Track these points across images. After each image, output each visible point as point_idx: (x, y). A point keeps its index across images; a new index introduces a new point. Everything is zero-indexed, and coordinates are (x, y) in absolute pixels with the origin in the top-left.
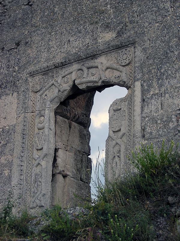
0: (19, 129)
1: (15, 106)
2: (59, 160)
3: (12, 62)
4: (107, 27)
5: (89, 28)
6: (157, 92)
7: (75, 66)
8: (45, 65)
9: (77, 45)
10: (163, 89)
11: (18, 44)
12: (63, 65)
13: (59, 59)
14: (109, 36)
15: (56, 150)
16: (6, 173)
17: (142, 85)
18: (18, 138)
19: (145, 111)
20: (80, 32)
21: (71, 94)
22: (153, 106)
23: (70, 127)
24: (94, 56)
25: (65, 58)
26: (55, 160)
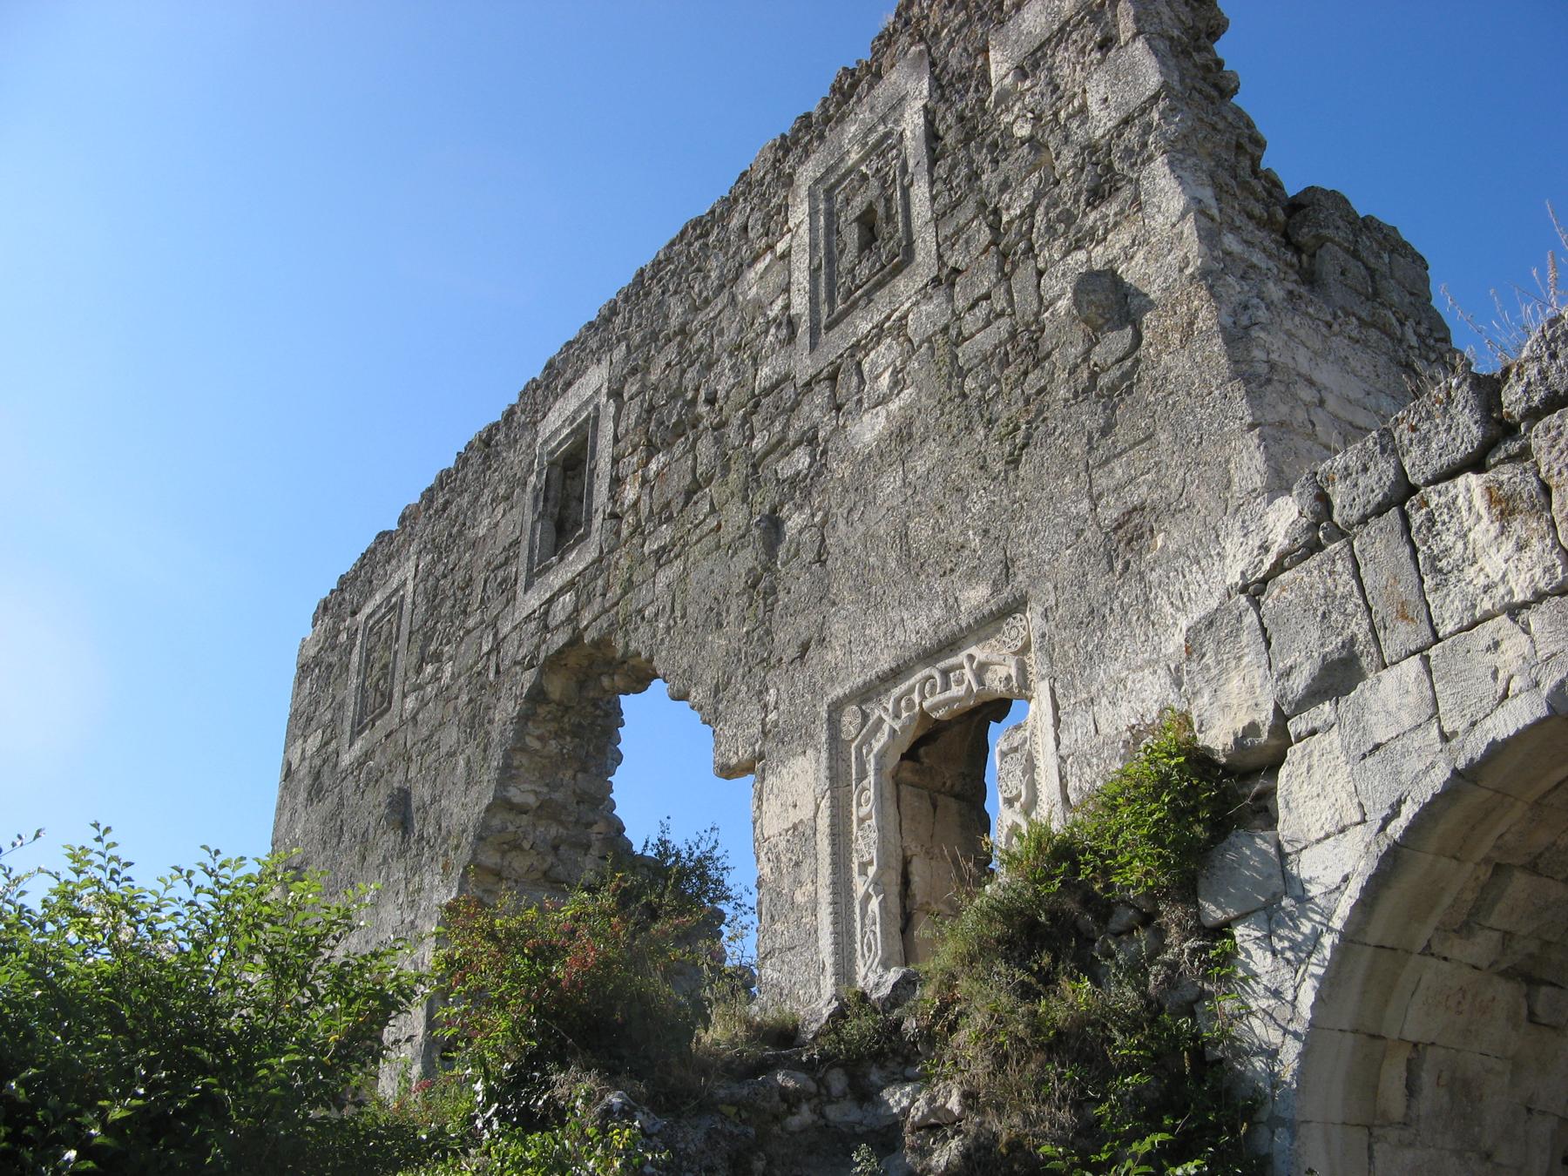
0: (824, 823)
1: (810, 778)
2: (916, 880)
3: (800, 685)
4: (972, 575)
6: (1084, 696)
8: (860, 681)
10: (1094, 689)
11: (805, 647)
12: (896, 674)
13: (885, 663)
14: (976, 596)
15: (906, 863)
17: (1052, 690)
19: (1065, 740)
20: (921, 598)
21: (920, 733)
23: (935, 807)
25: (897, 658)
26: (906, 881)
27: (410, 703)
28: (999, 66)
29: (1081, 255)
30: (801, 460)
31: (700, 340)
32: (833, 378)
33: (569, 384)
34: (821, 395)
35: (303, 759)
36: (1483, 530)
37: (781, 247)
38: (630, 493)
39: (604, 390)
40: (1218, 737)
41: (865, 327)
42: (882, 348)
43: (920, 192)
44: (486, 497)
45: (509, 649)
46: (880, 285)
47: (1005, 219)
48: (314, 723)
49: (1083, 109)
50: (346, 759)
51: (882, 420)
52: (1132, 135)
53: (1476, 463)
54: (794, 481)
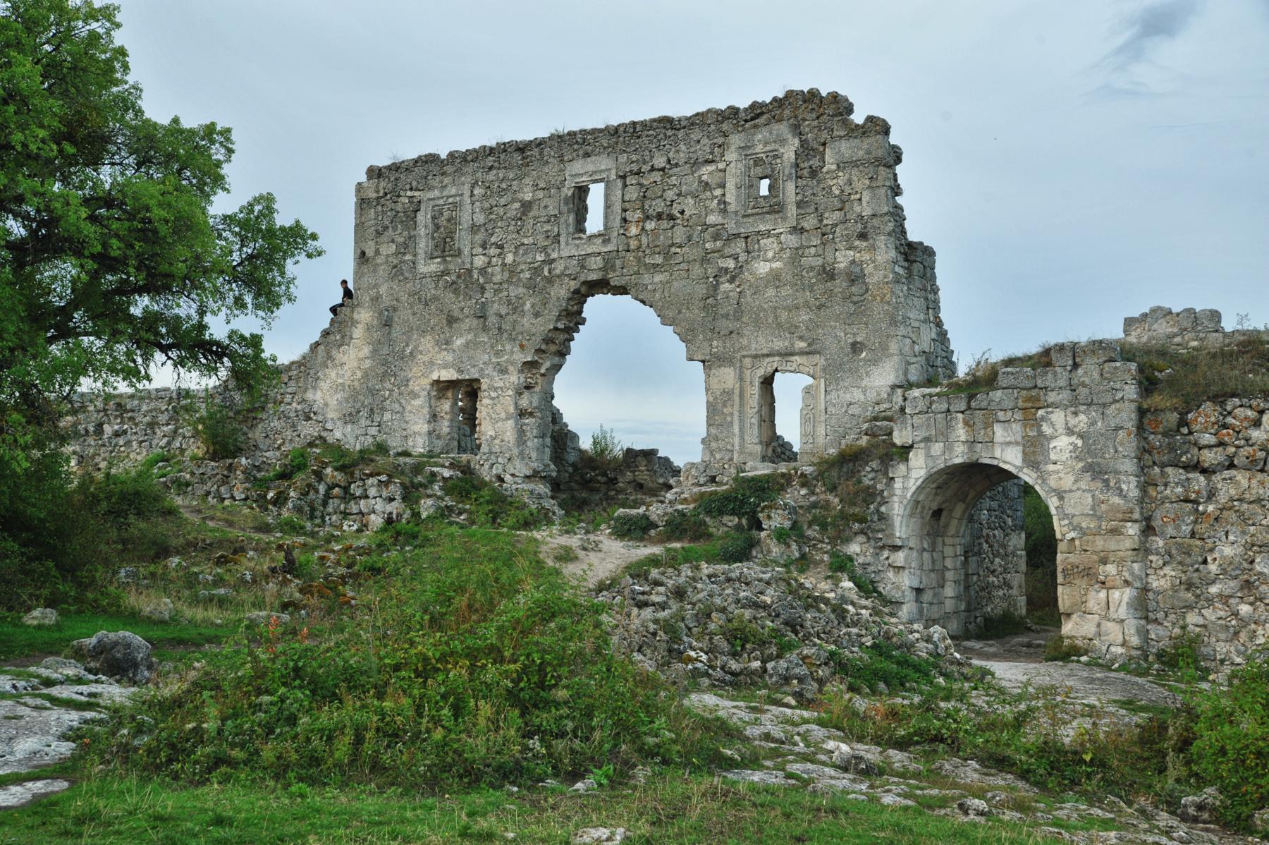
0: (737, 392)
4: (801, 338)
5: (788, 335)
7: (777, 358)
9: (779, 345)
13: (765, 351)
14: (803, 345)
16: (729, 419)
18: (736, 398)
22: (833, 395)
24: (792, 354)
27: (479, 261)
28: (829, 156)
29: (852, 253)
30: (731, 264)
31: (673, 180)
32: (746, 238)
33: (587, 155)
34: (741, 244)
35: (377, 252)
36: (961, 425)
37: (721, 166)
38: (634, 230)
39: (614, 172)
40: (897, 440)
41: (762, 228)
42: (771, 240)
43: (791, 187)
44: (527, 180)
45: (559, 267)
46: (768, 213)
47: (825, 222)
48: (385, 238)
49: (860, 199)
50: (423, 268)
51: (767, 269)
52: (875, 222)
53: (962, 412)
54: (727, 269)
